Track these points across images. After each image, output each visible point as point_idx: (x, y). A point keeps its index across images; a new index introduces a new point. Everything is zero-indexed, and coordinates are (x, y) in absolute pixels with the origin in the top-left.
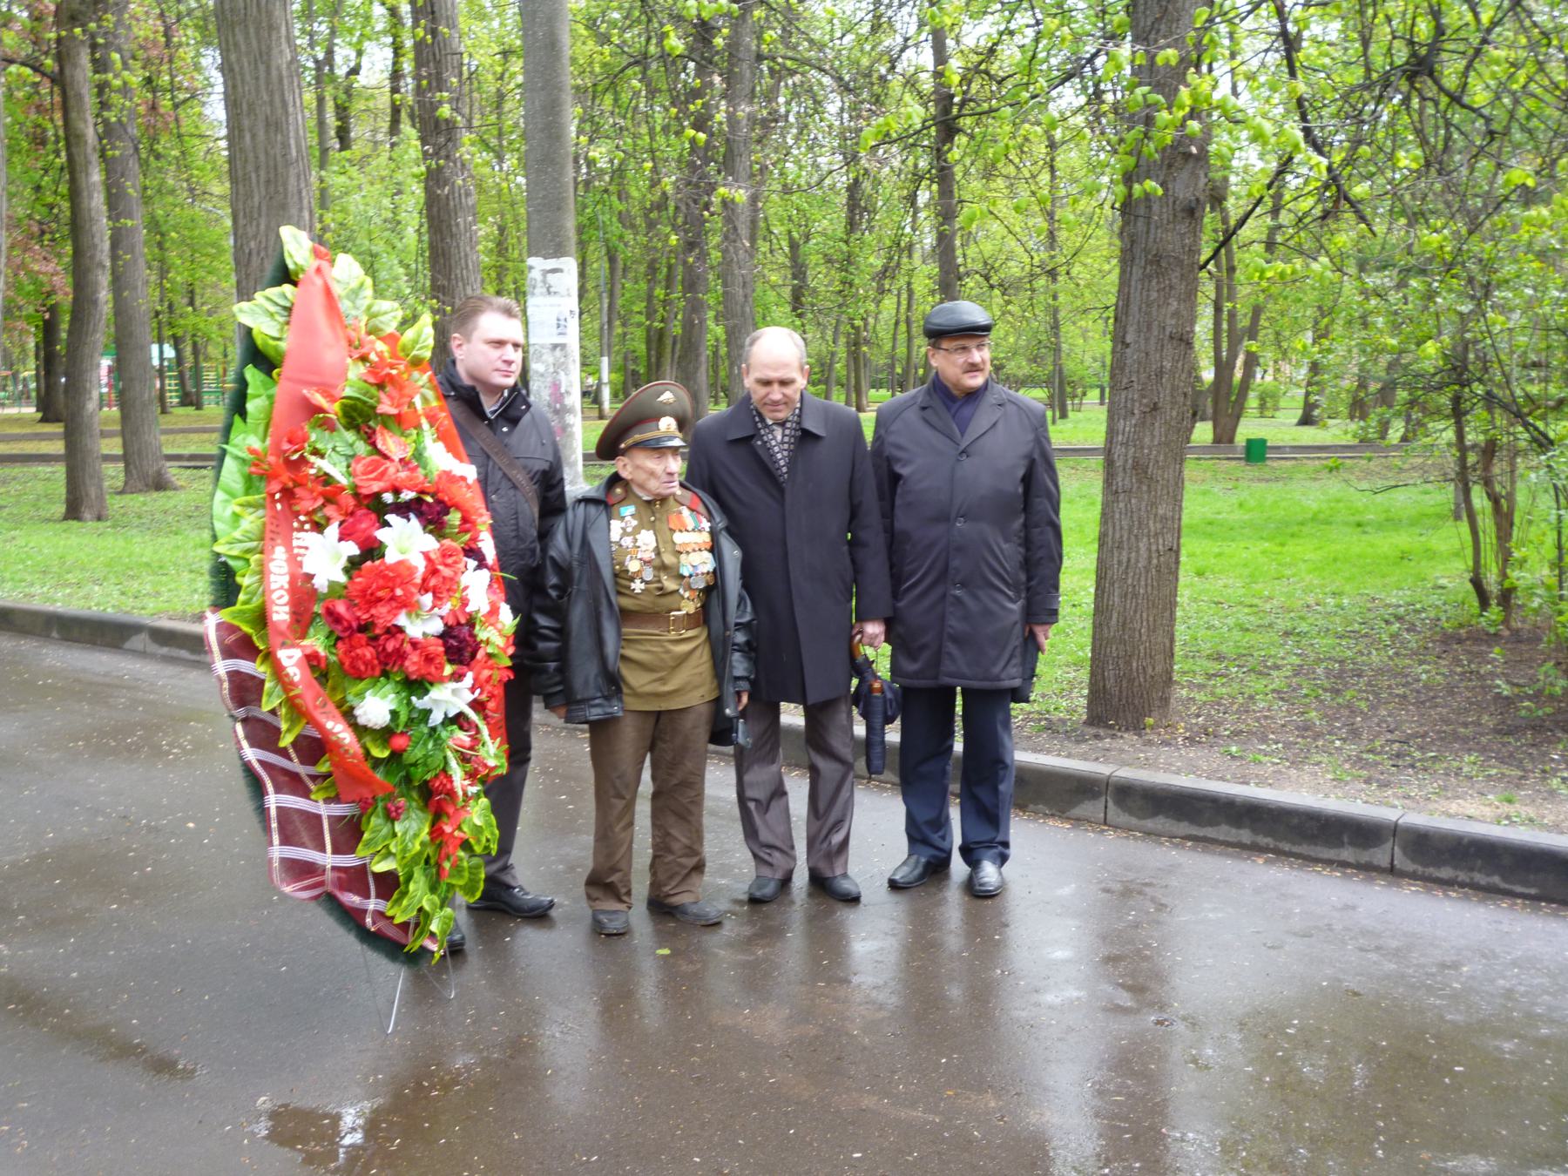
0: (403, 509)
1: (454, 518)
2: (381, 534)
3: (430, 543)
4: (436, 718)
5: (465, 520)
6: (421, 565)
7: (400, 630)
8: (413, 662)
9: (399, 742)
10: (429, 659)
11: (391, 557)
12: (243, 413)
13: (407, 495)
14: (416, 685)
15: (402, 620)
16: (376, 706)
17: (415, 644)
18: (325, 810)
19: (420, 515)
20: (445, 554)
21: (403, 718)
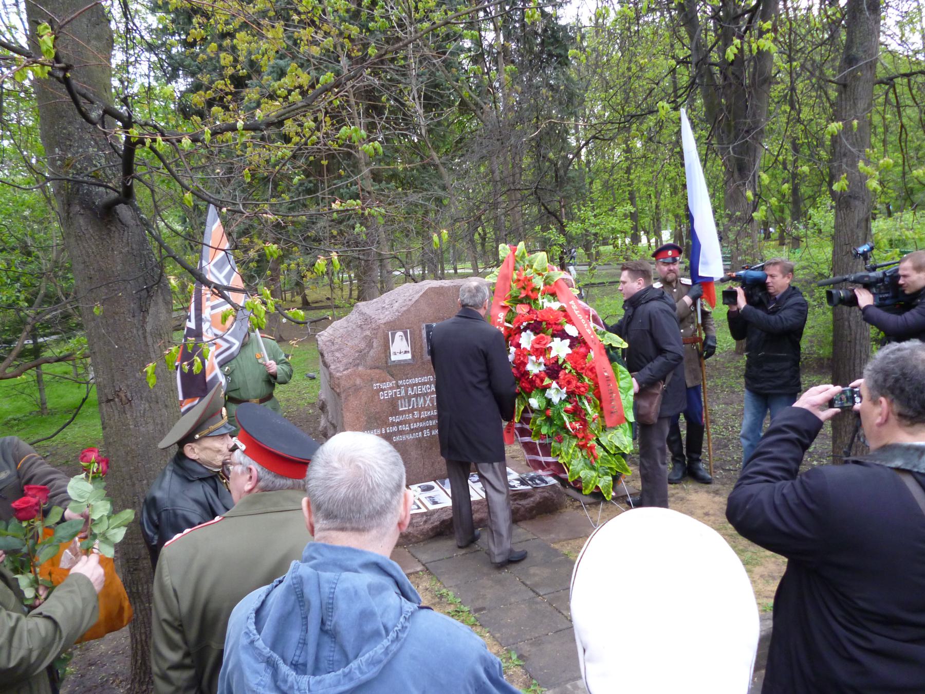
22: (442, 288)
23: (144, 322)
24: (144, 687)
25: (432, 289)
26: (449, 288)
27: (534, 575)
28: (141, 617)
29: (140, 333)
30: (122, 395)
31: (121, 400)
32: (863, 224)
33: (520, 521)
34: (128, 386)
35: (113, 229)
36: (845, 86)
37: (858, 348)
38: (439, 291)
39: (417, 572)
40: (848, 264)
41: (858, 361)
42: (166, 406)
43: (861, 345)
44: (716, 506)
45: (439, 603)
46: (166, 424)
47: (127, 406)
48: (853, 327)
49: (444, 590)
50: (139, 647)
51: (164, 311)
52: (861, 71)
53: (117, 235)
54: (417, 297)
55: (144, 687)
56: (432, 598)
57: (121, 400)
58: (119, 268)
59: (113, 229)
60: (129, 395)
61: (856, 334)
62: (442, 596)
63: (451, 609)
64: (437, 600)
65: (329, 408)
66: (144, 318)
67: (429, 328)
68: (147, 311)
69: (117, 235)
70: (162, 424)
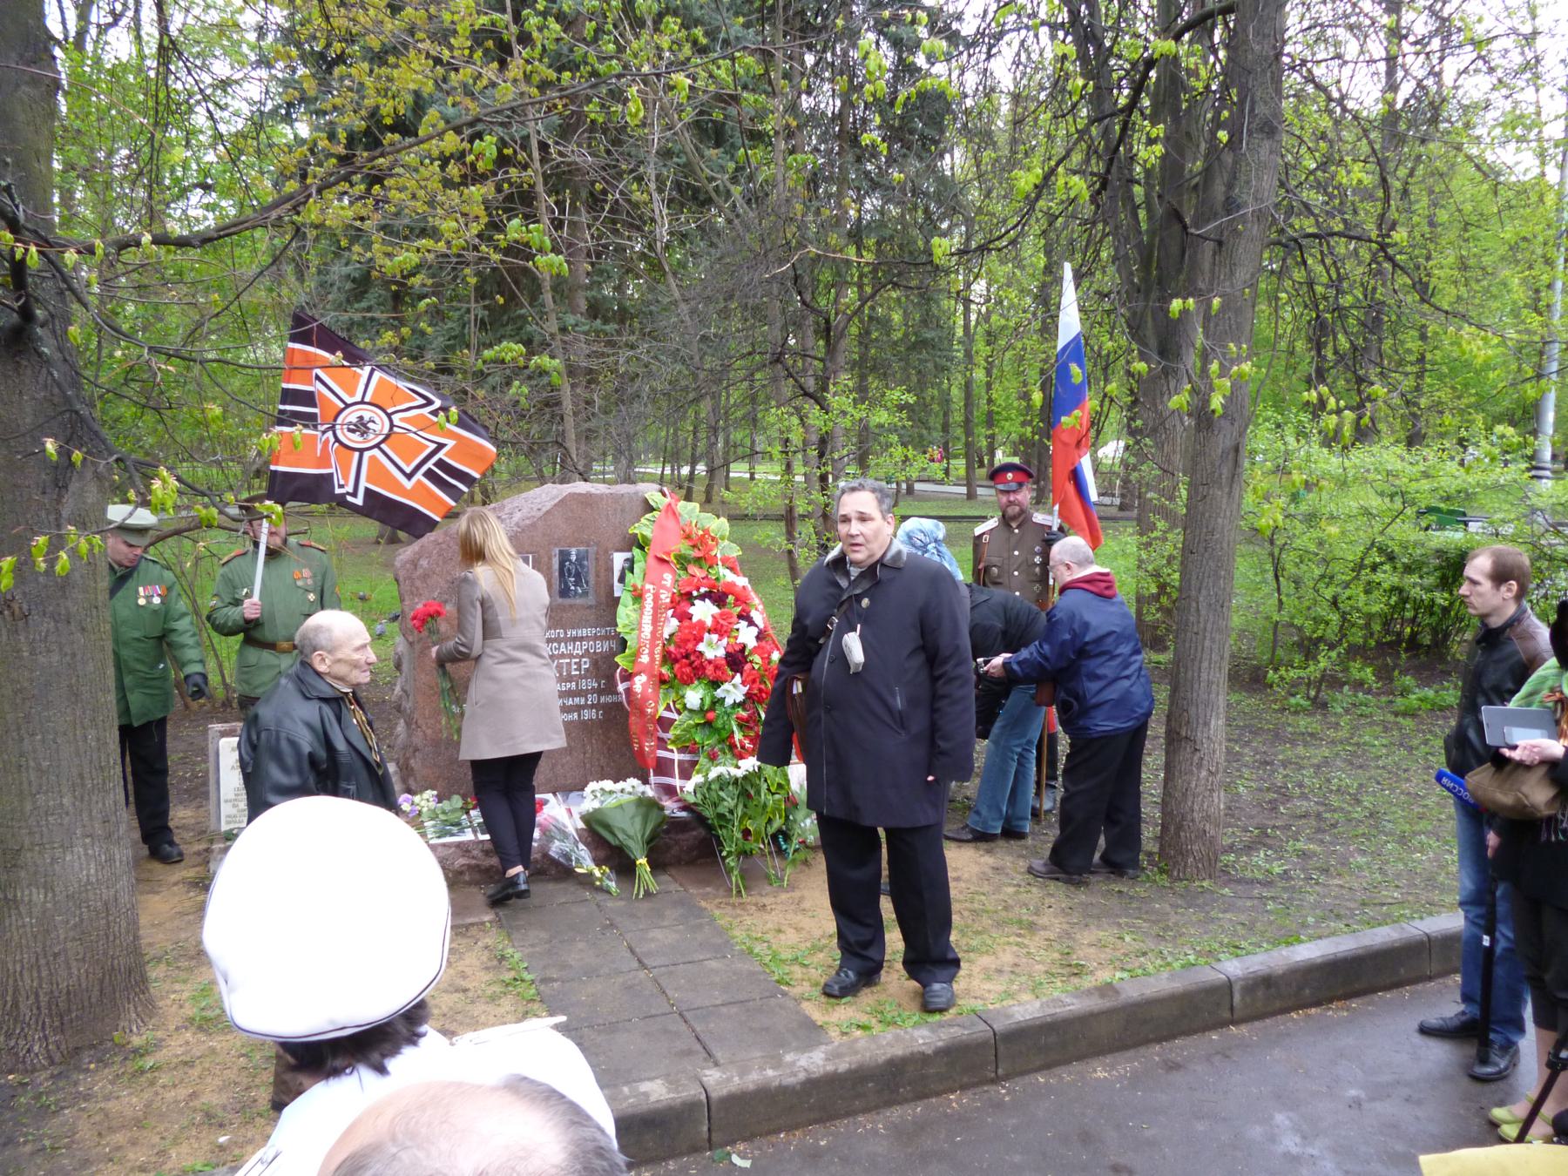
0: (702, 597)
1: (731, 599)
2: (692, 610)
3: (715, 610)
4: (729, 701)
5: (737, 600)
6: (709, 622)
7: (701, 654)
8: (710, 670)
9: (710, 715)
10: (717, 667)
11: (695, 620)
12: (632, 571)
13: (703, 590)
14: (715, 684)
15: (701, 647)
16: (694, 696)
17: (710, 662)
18: (677, 757)
19: (710, 598)
20: (721, 615)
21: (708, 702)
22: (589, 495)
23: (59, 501)
24: (12, 1043)
25: (572, 496)
26: (601, 497)
27: (653, 940)
28: (16, 938)
29: (52, 518)
30: (15, 606)
31: (13, 614)
32: (1231, 456)
33: (671, 864)
34: (24, 593)
35: (24, 363)
36: (1220, 243)
37: (1207, 643)
38: (586, 500)
39: (483, 923)
40: (1203, 514)
41: (1205, 664)
42: (83, 629)
43: (1213, 640)
44: (975, 869)
45: (495, 968)
46: (79, 657)
47: (21, 624)
48: (1203, 612)
49: (510, 951)
50: (11, 981)
51: (95, 489)
52: (1244, 223)
53: (29, 372)
54: (549, 506)
55: (12, 1043)
56: (490, 959)
57: (13, 614)
58: (28, 420)
59: (24, 363)
60: (25, 607)
61: (1206, 622)
62: (503, 958)
63: (508, 976)
64: (495, 963)
65: (405, 667)
66: (60, 496)
67: (564, 556)
68: (66, 487)
69: (29, 372)
70: (74, 655)
